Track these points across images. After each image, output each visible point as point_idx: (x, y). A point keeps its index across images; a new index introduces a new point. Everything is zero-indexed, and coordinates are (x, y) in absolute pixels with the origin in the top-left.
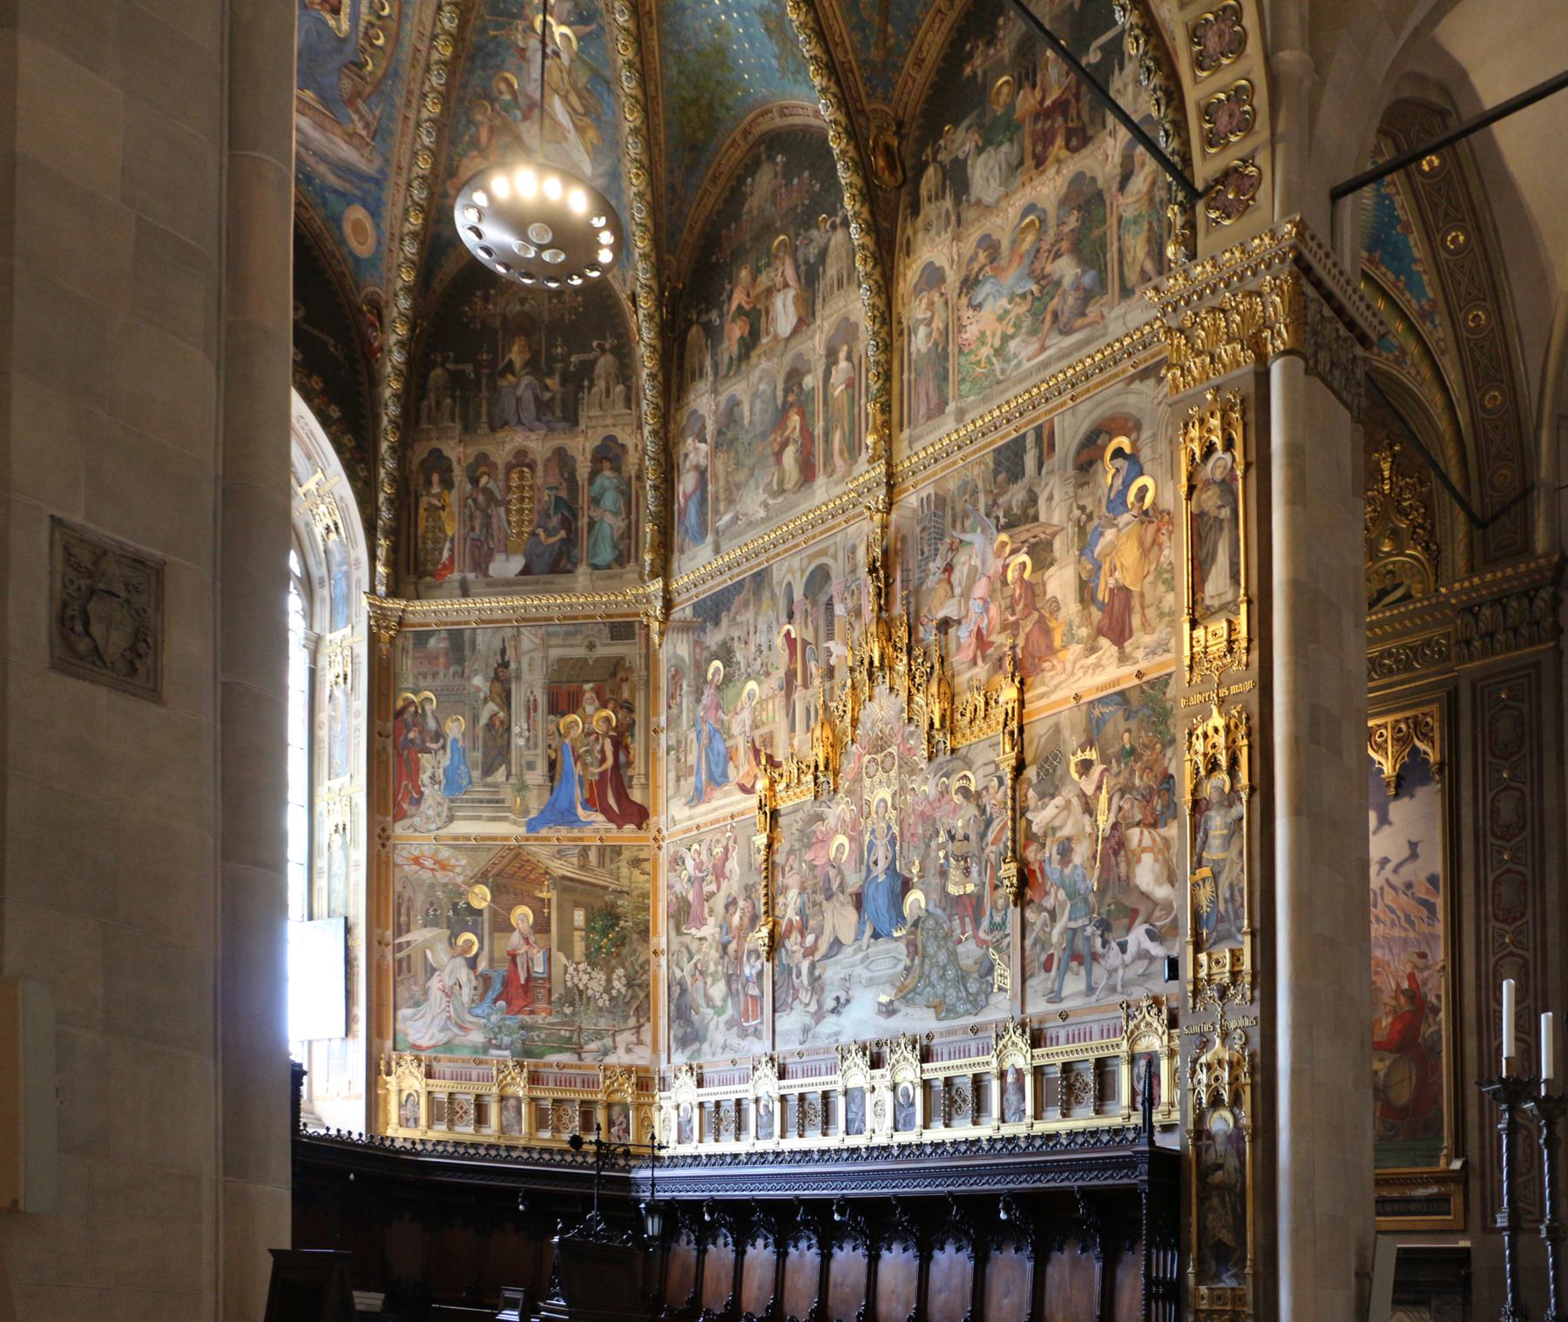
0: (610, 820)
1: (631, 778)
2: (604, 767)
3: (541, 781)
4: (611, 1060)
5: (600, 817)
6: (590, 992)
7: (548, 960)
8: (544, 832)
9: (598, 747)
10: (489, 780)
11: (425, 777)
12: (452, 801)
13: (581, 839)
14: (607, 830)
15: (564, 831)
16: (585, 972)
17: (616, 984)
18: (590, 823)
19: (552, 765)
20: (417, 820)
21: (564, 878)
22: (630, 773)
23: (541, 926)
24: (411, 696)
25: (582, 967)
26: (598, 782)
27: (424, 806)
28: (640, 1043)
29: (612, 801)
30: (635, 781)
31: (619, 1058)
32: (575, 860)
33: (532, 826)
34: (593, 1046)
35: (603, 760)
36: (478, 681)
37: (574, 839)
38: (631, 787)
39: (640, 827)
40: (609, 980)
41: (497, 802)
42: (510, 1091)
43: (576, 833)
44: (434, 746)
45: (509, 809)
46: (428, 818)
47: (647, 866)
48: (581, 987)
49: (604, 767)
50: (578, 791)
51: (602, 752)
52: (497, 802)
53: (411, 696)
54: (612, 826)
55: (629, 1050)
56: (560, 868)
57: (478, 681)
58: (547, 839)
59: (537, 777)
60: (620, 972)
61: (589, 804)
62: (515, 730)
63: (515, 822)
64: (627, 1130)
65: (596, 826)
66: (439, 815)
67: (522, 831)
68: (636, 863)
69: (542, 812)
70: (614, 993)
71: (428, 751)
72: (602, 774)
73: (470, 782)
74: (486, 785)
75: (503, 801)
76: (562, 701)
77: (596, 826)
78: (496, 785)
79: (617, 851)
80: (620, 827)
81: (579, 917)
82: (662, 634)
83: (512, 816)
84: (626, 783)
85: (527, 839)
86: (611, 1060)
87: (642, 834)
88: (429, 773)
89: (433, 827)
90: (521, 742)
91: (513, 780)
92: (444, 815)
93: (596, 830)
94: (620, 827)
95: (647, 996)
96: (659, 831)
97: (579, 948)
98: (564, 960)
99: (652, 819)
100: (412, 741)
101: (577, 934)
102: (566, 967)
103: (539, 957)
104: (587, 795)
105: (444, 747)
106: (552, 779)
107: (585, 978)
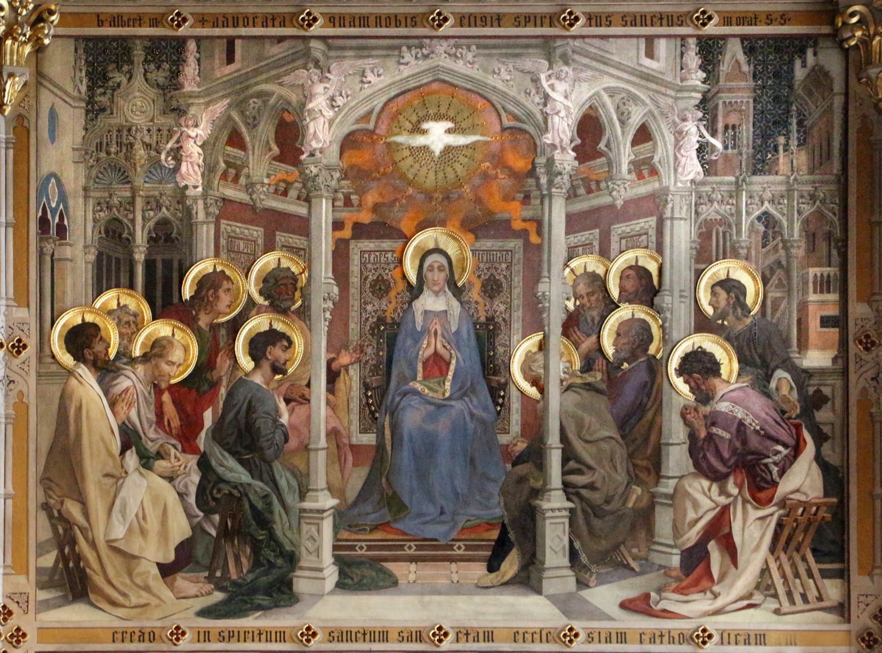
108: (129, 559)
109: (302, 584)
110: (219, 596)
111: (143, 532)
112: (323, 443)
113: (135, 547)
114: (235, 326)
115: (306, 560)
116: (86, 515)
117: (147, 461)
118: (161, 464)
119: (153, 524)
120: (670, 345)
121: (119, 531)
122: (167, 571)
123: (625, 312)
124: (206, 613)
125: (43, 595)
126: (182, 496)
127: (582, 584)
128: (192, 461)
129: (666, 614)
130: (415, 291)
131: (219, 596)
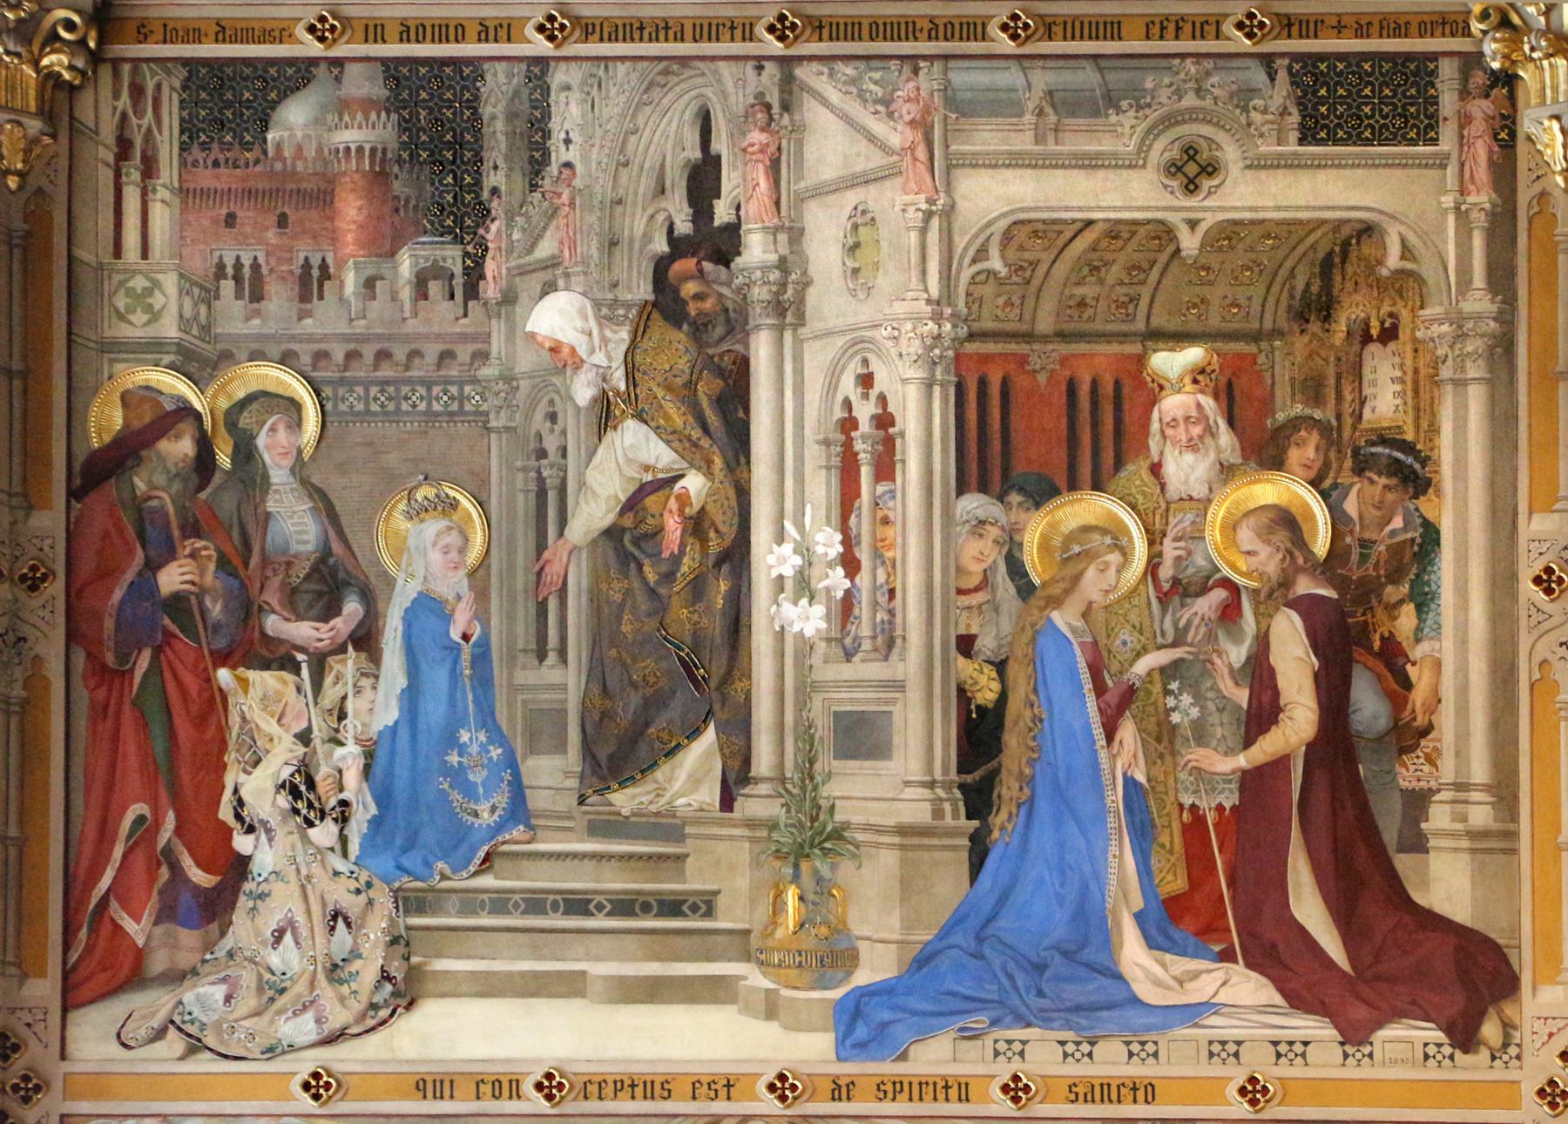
0: (1297, 1000)
1: (1418, 802)
3: (915, 809)
10: (624, 800)
12: (409, 902)
14: (1280, 1049)
18: (1193, 1013)
20: (203, 998)
22: (1410, 774)
26: (1236, 820)
27: (245, 929)
30: (1439, 817)
38: (1417, 843)
39: (1464, 1037)
41: (672, 906)
44: (304, 631)
45: (741, 944)
46: (273, 990)
50: (1122, 861)
52: (672, 906)
63: (771, 1009)
66: (334, 971)
69: (924, 960)
71: (281, 658)
72: (1258, 783)
73: (518, 810)
74: (598, 829)
75: (706, 905)
77: (1220, 1026)
78: (667, 827)
80: (1354, 1035)
83: (755, 978)
84: (1390, 830)
85: (841, 1090)
87: (1474, 1067)
88: (280, 760)
89: (303, 1028)
91: (756, 804)
92: (368, 971)
93: (1232, 1050)
94: (1354, 1035)
100: (177, 604)
104: (1177, 883)
105: (365, 640)
106: (979, 800)
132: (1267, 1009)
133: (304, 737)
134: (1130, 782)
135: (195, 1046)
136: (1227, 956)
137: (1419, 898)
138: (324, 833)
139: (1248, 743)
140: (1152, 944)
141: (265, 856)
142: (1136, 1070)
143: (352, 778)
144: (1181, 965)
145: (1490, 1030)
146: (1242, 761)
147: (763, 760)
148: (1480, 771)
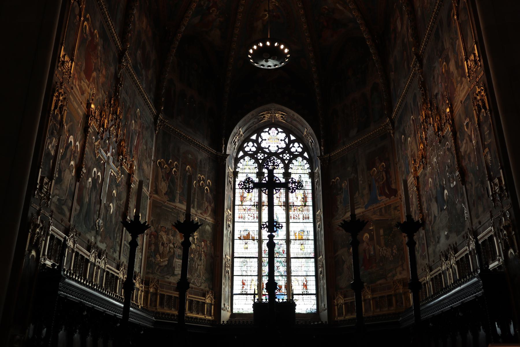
0: (387, 197)
2: (384, 181)
4: (395, 278)
5: (384, 197)
6: (387, 256)
7: (374, 249)
8: (369, 208)
9: (381, 175)
11: (338, 203)
13: (379, 206)
14: (386, 201)
15: (375, 206)
16: (385, 250)
17: (394, 251)
18: (381, 200)
19: (370, 186)
21: (376, 220)
23: (371, 238)
24: (333, 180)
25: (384, 248)
28: (403, 270)
29: (387, 191)
30: (393, 182)
31: (399, 277)
32: (378, 214)
33: (366, 207)
34: (390, 275)
35: (383, 179)
36: (349, 169)
37: (378, 207)
39: (395, 196)
40: (392, 250)
42: (366, 297)
43: (378, 205)
47: (399, 208)
48: (384, 255)
49: (384, 181)
51: (383, 176)
53: (333, 180)
54: (388, 199)
55: (400, 273)
56: (375, 217)
57: (349, 169)
58: (370, 210)
59: (366, 192)
60: (395, 246)
61: (381, 195)
62: (360, 179)
63: (362, 208)
64: (402, 303)
65: (383, 200)
67: (364, 210)
68: (395, 208)
70: (394, 254)
76: (371, 165)
77: (383, 200)
79: (390, 206)
80: (390, 198)
81: (382, 232)
82: (393, 133)
86: (395, 278)
88: (339, 201)
89: (341, 217)
90: (361, 182)
93: (383, 202)
94: (390, 198)
95: (404, 253)
96: (401, 195)
97: (382, 242)
98: (379, 248)
99: (399, 192)
101: (381, 237)
102: (380, 250)
103: (372, 248)
105: (342, 192)
107: (385, 251)
108: (162, 191)
109: (176, 201)
110: (169, 199)
111: (163, 189)
112: (179, 185)
113: (162, 190)
114: (173, 168)
115: (176, 198)
116: (158, 185)
117: (164, 180)
118: (165, 181)
119: (164, 188)
120: (205, 187)
121: (161, 188)
122: (165, 194)
123: (202, 182)
124: (167, 200)
125: (154, 192)
126: (167, 186)
127: (197, 210)
128: (168, 182)
129: (203, 215)
130: (187, 172)
131: (169, 199)
132: (385, 198)
133: (340, 199)
134: (377, 186)
135: (337, 220)
136: (383, 196)
137: (392, 188)
138: (341, 205)
139: (382, 181)
140: (379, 196)
141: (339, 207)
142: (379, 205)
143: (342, 201)
144: (381, 197)
145: (397, 195)
146: (382, 182)
147: (360, 192)
148: (394, 178)
